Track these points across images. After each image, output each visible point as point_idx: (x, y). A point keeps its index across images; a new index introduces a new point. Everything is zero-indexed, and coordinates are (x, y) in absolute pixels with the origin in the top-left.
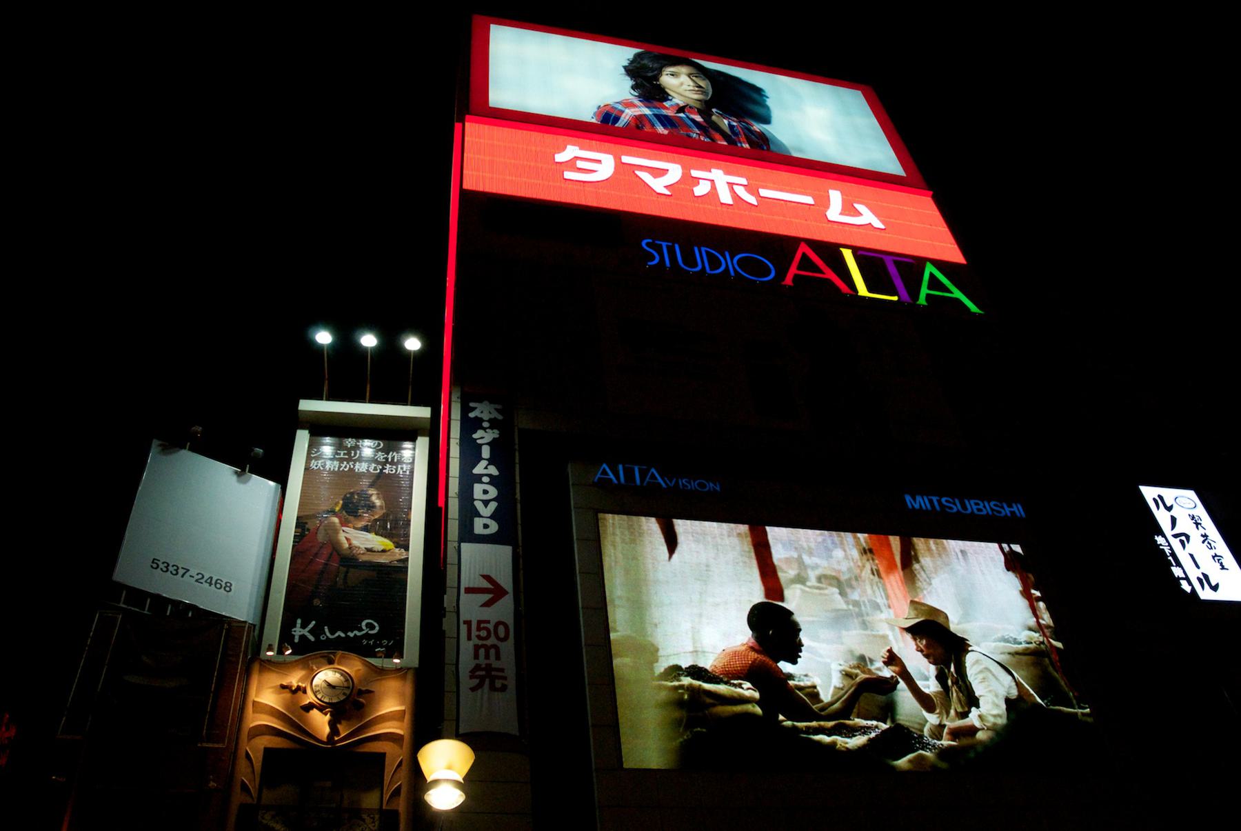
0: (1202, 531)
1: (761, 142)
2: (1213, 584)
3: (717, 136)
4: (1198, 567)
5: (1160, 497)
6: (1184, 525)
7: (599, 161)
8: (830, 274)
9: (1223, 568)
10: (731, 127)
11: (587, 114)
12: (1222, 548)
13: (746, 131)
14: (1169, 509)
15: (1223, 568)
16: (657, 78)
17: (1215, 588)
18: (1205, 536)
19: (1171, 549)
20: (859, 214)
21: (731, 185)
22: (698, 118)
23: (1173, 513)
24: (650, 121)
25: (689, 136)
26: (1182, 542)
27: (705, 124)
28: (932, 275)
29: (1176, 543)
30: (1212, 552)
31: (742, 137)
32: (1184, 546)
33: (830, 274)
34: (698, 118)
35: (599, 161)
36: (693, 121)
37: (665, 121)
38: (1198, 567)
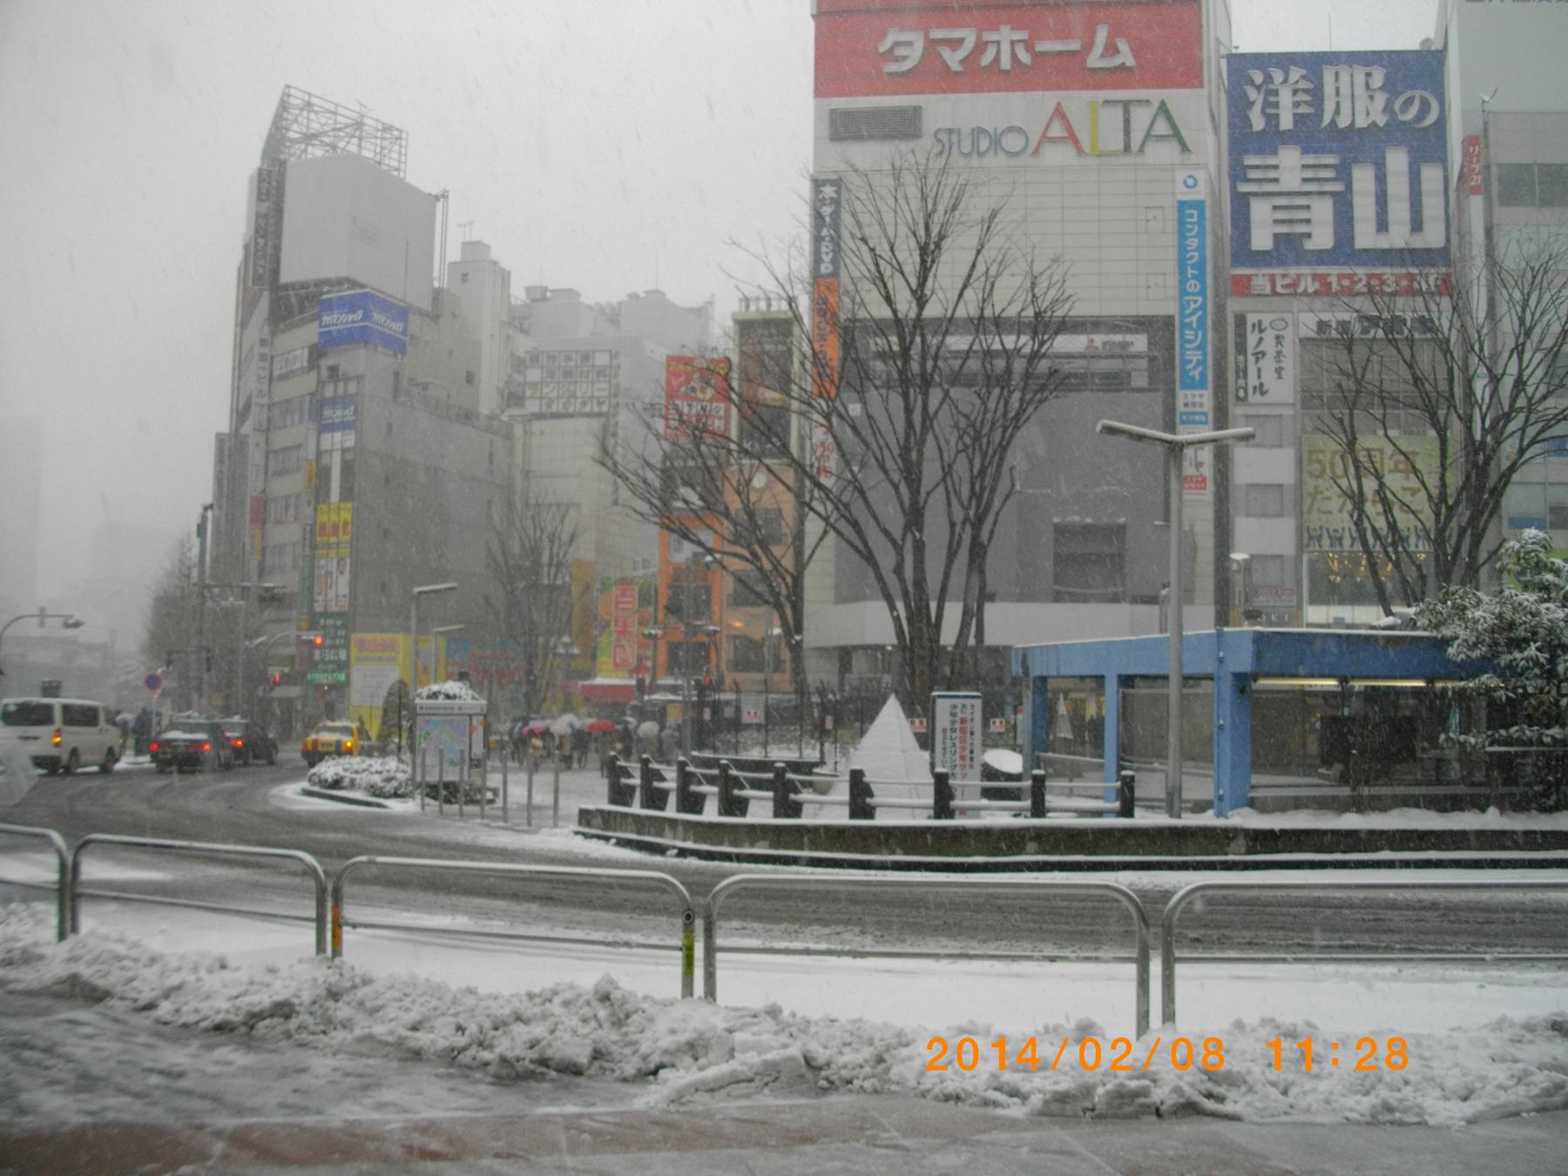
0: (1279, 348)
2: (1265, 389)
4: (1259, 377)
5: (1260, 322)
6: (1269, 346)
7: (910, 44)
9: (1280, 377)
12: (1289, 363)
14: (1261, 331)
15: (1280, 377)
17: (1263, 393)
18: (1279, 353)
19: (1246, 367)
20: (1117, 51)
21: (1013, 43)
23: (1264, 335)
26: (1257, 360)
29: (1251, 359)
30: (1277, 365)
32: (1257, 360)
35: (910, 44)
38: (1259, 377)
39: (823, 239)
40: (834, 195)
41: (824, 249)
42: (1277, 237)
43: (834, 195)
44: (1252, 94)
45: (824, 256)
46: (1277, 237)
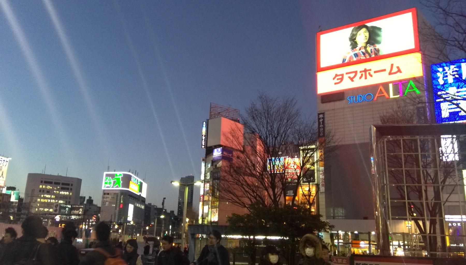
1: (377, 52)
3: (367, 55)
8: (385, 94)
10: (371, 50)
11: (340, 62)
13: (375, 50)
16: (355, 39)
22: (364, 50)
24: (353, 57)
25: (361, 58)
27: (365, 52)
28: (411, 85)
31: (373, 53)
33: (385, 94)
34: (364, 50)
36: (362, 52)
37: (356, 55)
39: (320, 127)
40: (323, 117)
41: (321, 130)
42: (451, 113)
43: (323, 117)
44: (439, 74)
45: (321, 132)
46: (451, 113)
